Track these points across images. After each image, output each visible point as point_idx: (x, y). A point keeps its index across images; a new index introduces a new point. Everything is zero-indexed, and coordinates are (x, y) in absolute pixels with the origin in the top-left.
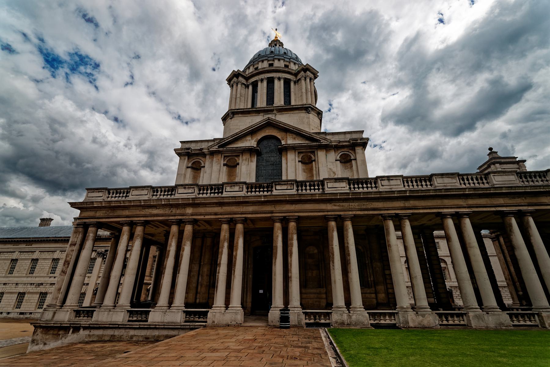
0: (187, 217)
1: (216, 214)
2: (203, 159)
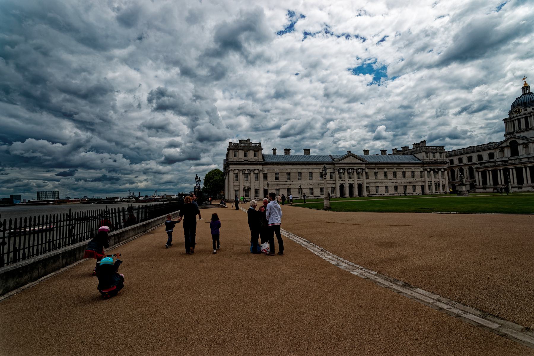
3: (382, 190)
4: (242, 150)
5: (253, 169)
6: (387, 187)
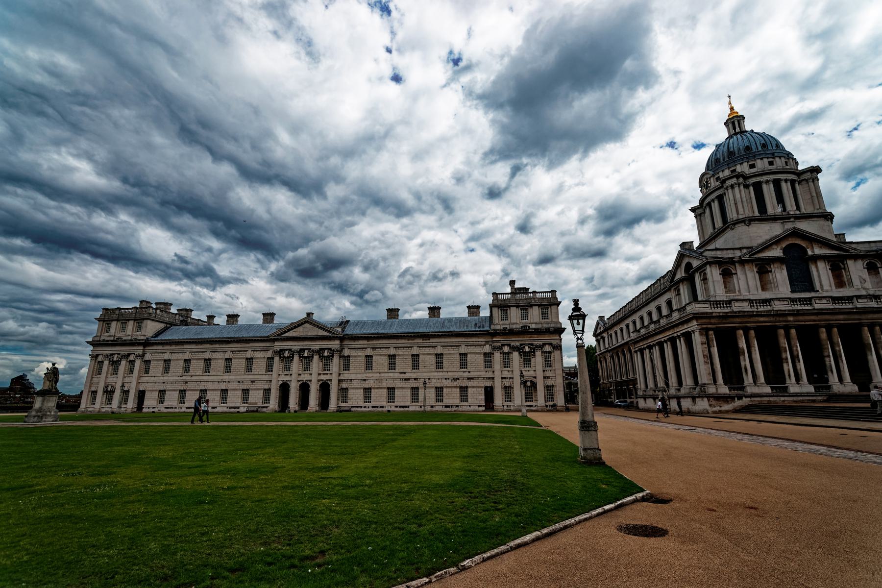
0: (791, 323)
1: (814, 321)
2: (733, 267)
3: (379, 398)
4: (118, 320)
5: (126, 353)
6: (391, 390)
